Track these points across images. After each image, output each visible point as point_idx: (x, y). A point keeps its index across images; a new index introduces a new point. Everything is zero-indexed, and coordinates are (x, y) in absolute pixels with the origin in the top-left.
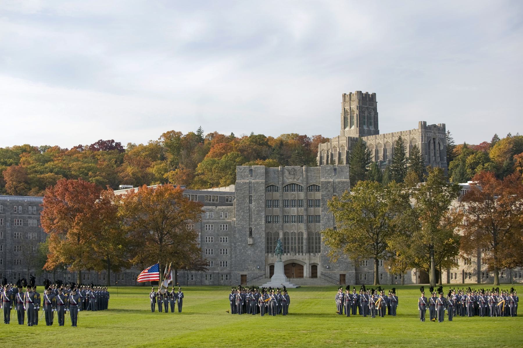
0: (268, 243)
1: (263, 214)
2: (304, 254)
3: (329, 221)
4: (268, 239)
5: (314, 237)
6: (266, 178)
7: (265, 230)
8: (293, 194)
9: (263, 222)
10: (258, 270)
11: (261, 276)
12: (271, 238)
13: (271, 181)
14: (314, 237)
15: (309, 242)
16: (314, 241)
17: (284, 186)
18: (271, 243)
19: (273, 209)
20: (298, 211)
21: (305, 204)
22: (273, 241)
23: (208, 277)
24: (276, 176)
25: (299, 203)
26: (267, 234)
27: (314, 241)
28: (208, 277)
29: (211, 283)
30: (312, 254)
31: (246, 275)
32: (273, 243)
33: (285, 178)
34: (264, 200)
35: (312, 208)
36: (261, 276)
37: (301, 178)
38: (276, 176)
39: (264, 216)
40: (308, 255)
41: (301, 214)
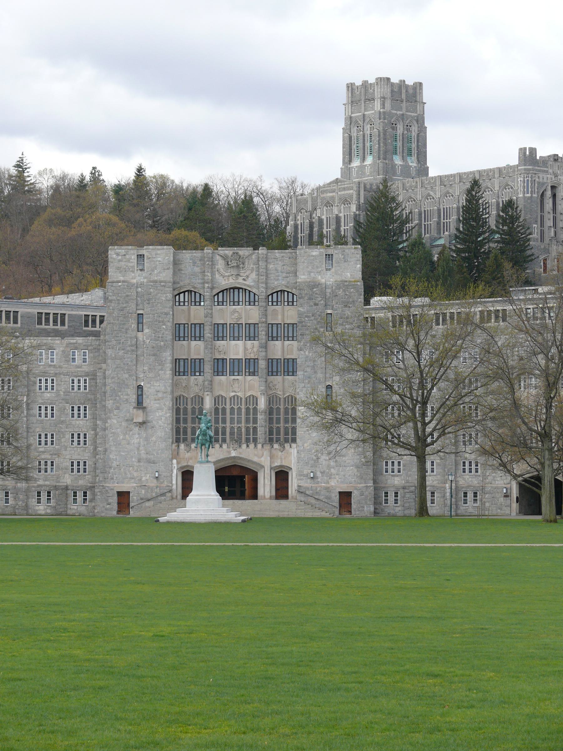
0: (178, 421)
1: (167, 356)
2: (259, 446)
3: (315, 372)
4: (178, 411)
5: (282, 407)
6: (174, 273)
7: (172, 392)
8: (235, 311)
9: (168, 373)
10: (155, 481)
11: (163, 494)
12: (185, 409)
13: (187, 281)
14: (282, 407)
15: (271, 420)
16: (282, 416)
17: (215, 291)
18: (185, 421)
19: (189, 345)
20: (245, 349)
21: (262, 334)
22: (189, 417)
23: (44, 497)
24: (197, 269)
25: (249, 332)
26: (177, 400)
27: (282, 416)
28: (44, 497)
29: (49, 511)
30: (276, 446)
31: (128, 493)
32: (189, 420)
33: (217, 276)
34: (169, 324)
35: (278, 343)
36: (163, 494)
37: (253, 276)
38: (197, 269)
39: (170, 358)
40: (268, 447)
41: (252, 356)
